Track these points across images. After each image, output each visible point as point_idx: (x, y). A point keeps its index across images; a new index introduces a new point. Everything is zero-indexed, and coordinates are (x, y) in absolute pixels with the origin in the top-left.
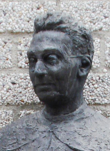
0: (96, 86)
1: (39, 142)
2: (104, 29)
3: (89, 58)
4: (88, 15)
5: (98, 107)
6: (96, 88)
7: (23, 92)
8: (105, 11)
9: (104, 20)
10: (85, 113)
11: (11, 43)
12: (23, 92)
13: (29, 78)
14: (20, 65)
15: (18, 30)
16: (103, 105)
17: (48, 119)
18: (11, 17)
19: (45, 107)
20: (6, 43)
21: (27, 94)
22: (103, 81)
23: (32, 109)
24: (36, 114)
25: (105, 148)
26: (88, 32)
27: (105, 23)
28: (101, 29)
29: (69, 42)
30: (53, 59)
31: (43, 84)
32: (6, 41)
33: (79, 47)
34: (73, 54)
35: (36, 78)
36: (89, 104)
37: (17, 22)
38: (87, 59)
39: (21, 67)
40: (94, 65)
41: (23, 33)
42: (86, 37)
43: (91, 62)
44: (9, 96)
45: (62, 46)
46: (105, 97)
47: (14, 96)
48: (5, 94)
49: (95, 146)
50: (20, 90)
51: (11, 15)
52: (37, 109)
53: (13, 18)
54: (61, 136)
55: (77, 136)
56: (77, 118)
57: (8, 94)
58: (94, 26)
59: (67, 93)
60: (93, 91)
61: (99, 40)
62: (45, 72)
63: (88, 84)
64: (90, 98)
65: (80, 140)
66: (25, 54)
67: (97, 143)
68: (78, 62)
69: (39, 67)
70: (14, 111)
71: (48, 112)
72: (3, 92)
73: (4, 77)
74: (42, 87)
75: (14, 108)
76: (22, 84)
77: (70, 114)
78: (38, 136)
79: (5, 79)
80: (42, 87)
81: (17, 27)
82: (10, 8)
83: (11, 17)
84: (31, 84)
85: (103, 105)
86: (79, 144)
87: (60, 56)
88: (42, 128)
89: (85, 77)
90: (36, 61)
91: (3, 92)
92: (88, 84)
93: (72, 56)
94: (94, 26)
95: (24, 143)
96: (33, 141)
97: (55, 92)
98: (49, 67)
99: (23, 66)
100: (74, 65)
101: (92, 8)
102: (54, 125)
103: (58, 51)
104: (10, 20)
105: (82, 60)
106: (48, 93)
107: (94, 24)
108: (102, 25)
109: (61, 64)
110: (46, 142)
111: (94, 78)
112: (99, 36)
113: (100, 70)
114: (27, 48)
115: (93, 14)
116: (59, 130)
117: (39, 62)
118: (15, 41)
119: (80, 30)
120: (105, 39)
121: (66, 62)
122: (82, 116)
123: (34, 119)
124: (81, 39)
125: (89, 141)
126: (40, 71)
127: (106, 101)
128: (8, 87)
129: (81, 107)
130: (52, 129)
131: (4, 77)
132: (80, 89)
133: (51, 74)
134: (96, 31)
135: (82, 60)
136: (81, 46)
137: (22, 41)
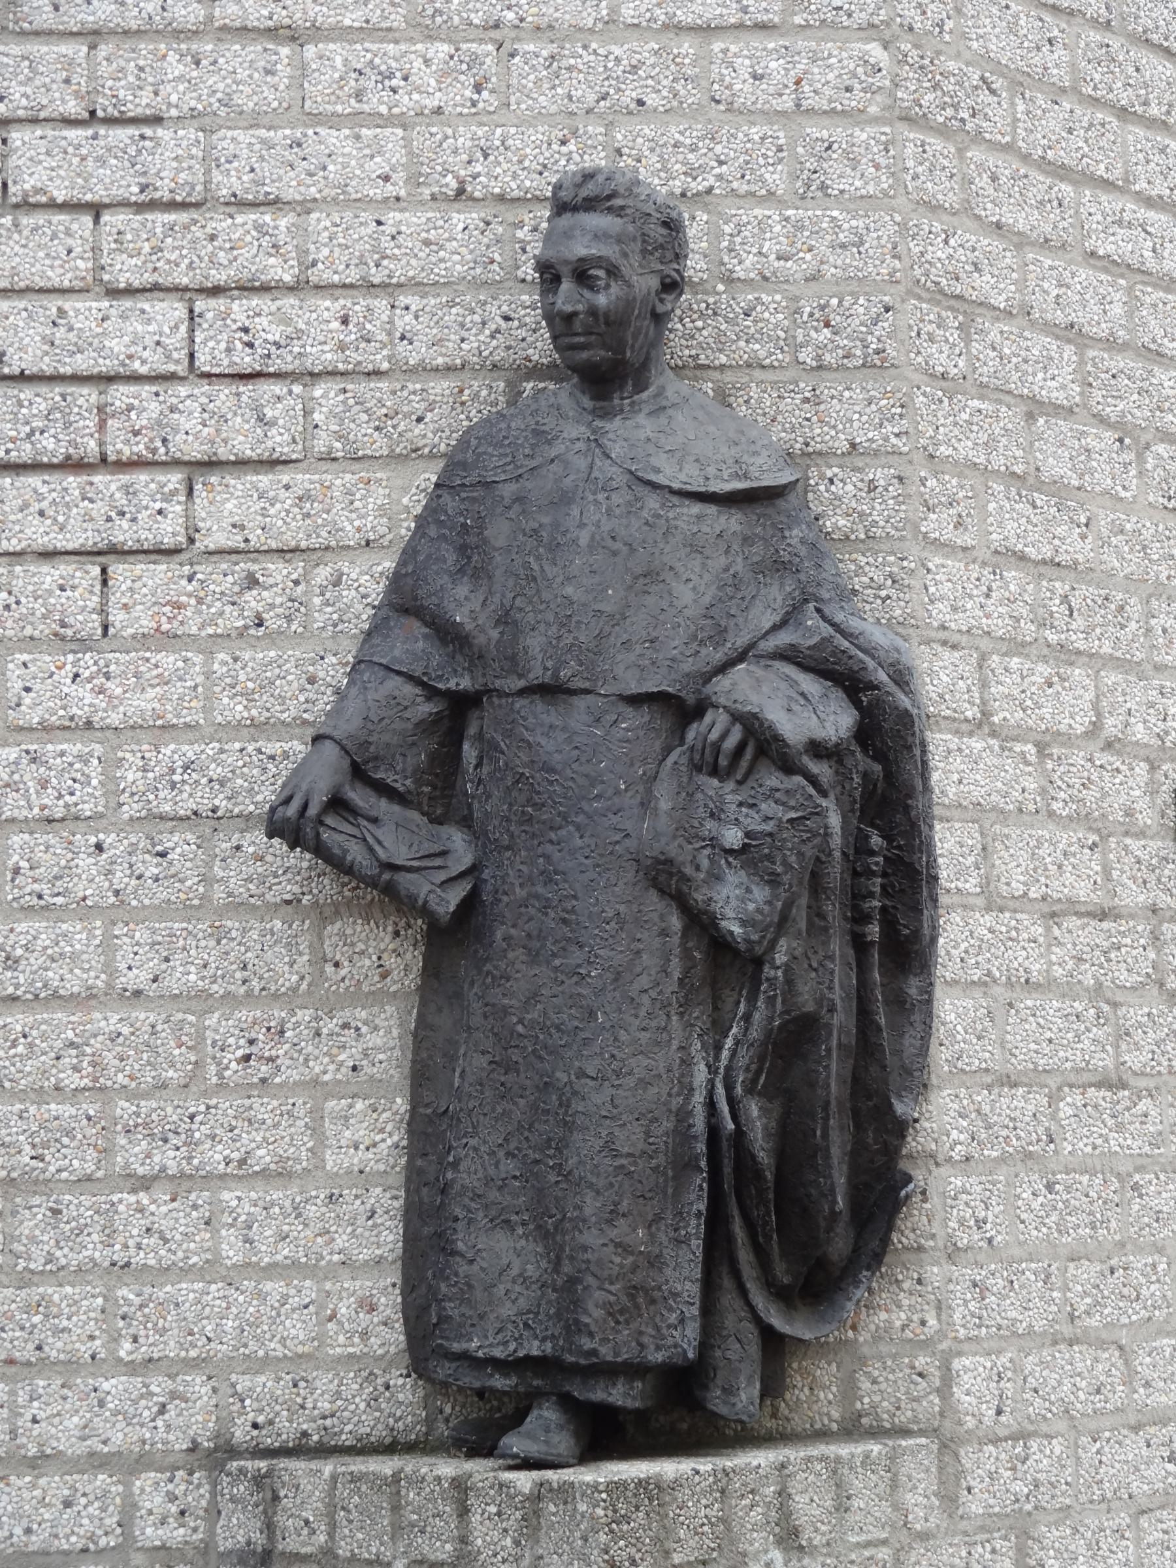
0: (700, 324)
1: (566, 463)
4: (680, 157)
5: (705, 374)
6: (699, 330)
8: (718, 149)
9: (717, 171)
14: (520, 274)
15: (516, 194)
16: (715, 368)
18: (499, 164)
20: (488, 223)
28: (709, 191)
37: (515, 176)
39: (523, 281)
46: (721, 351)
47: (508, 348)
50: (522, 333)
51: (501, 159)
53: (505, 166)
60: (693, 337)
64: (687, 352)
72: (482, 338)
73: (485, 303)
76: (527, 320)
81: (514, 186)
82: (497, 143)
85: (715, 368)
91: (482, 338)
92: (681, 320)
94: (693, 185)
99: (529, 278)
104: (499, 170)
107: (695, 179)
108: (712, 181)
111: (695, 307)
115: (690, 156)
127: (723, 359)
128: (494, 327)
131: (485, 303)
137: (527, 221)
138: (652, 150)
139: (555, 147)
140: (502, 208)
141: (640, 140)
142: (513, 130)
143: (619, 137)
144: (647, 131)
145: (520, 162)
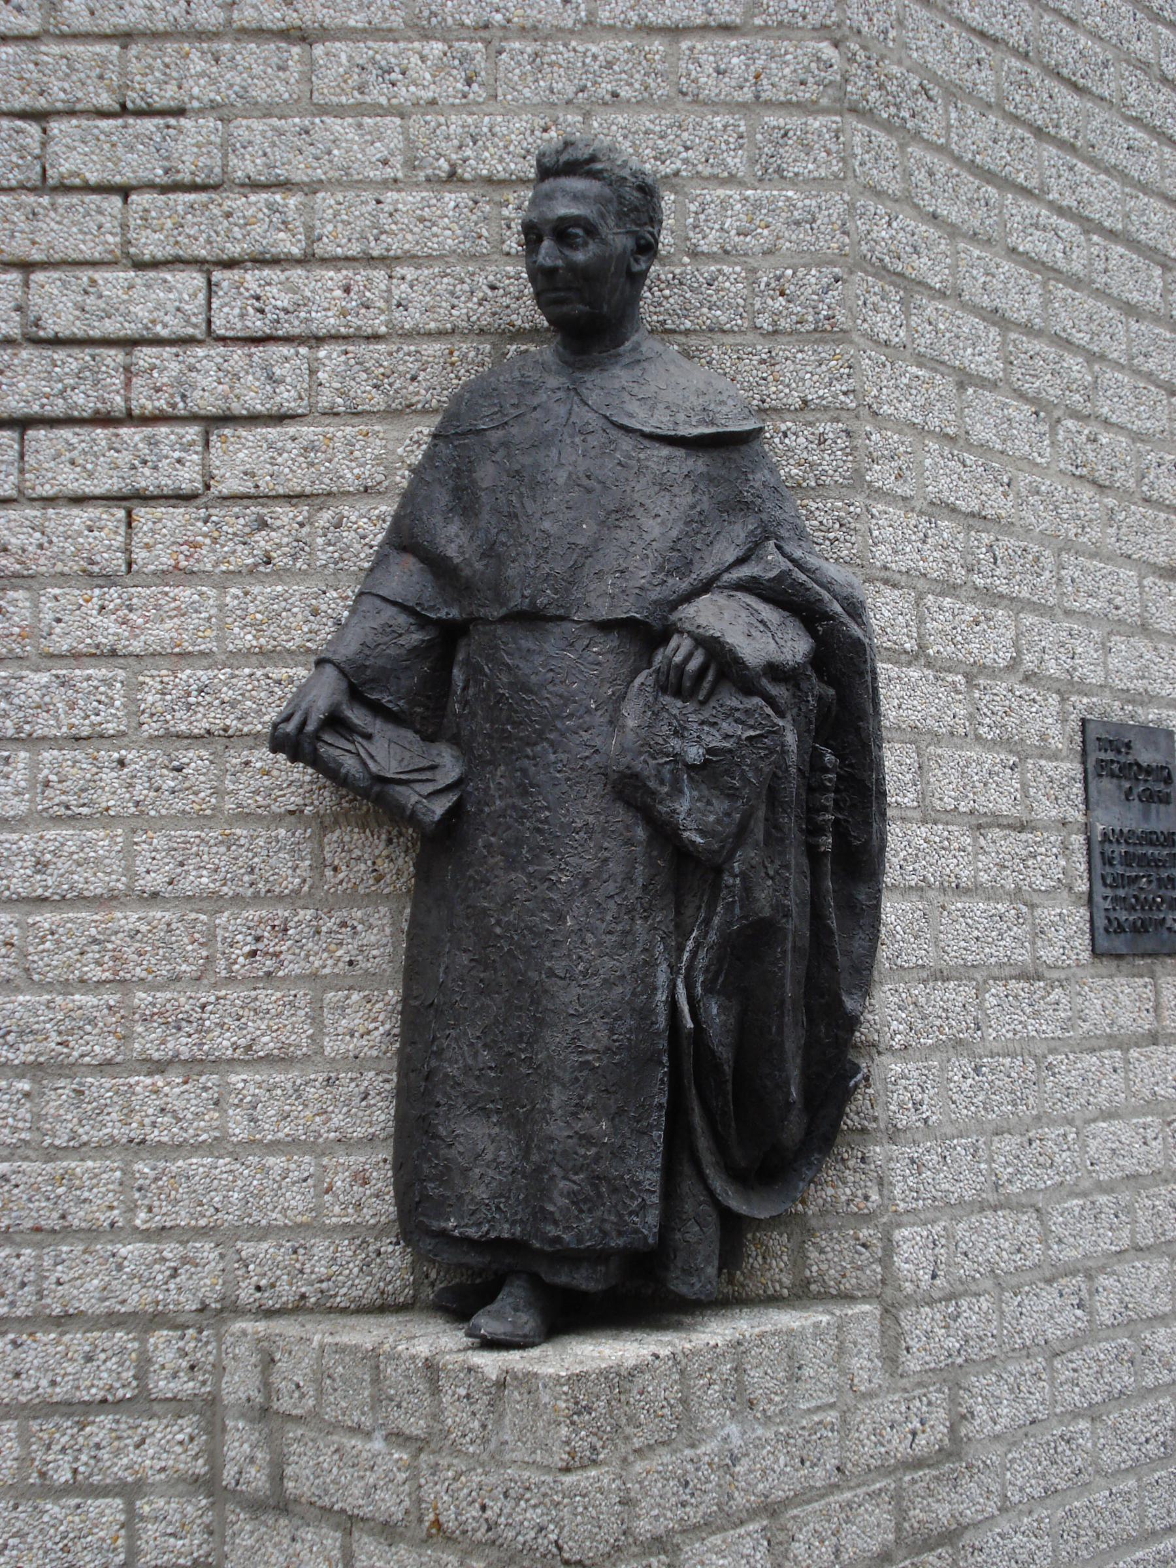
0: (667, 292)
2: (684, 174)
3: (652, 234)
4: (650, 143)
5: (671, 337)
6: (666, 298)
7: (514, 306)
8: (685, 135)
9: (684, 155)
10: (644, 349)
11: (488, 202)
12: (514, 306)
13: (525, 275)
14: (505, 248)
15: (502, 175)
16: (681, 333)
17: (565, 362)
18: (487, 149)
19: (558, 338)
20: (476, 203)
21: (522, 311)
22: (681, 283)
23: (532, 341)
24: (541, 352)
25: (685, 423)
26: (649, 181)
27: (686, 161)
28: (677, 174)
29: (610, 201)
30: (577, 236)
31: (556, 289)
32: (478, 198)
33: (631, 211)
34: (617, 226)
35: (539, 276)
36: (652, 332)
37: (501, 160)
38: (648, 236)
39: (508, 254)
40: (663, 250)
41: (512, 181)
42: (647, 191)
43: (657, 242)
44: (483, 314)
45: (594, 209)
46: (686, 317)
47: (494, 314)
48: (475, 311)
49: (664, 419)
50: (506, 301)
51: (489, 144)
52: (542, 342)
53: (492, 150)
54: (593, 398)
55: (627, 397)
56: (627, 361)
57: (481, 309)
58: (662, 167)
59: (605, 308)
60: (660, 305)
61: (672, 197)
62: (560, 263)
63: (650, 289)
64: (655, 318)
65: (633, 406)
66: (516, 226)
67: (668, 412)
68: (630, 243)
69: (547, 254)
70: (493, 345)
71: (565, 348)
72: (470, 305)
73: (473, 274)
74: (553, 295)
75: (495, 339)
76: (512, 288)
77: (612, 352)
78: (545, 397)
79: (476, 278)
80: (553, 295)
81: (500, 168)
82: (485, 130)
83: (487, 149)
84: (529, 290)
85: (681, 333)
86: (631, 416)
87: (591, 230)
88: (553, 382)
89: (644, 274)
90: (540, 240)
91: (470, 305)
92: (650, 289)
93: (616, 230)
94: (662, 167)
95: (514, 412)
96: (535, 409)
97: (581, 307)
98: (567, 252)
99: (513, 251)
100: (620, 250)
101: (658, 129)
102: (578, 375)
103: (586, 219)
104: (486, 154)
105: (638, 238)
106: (565, 309)
107: (663, 163)
108: (679, 164)
109: (593, 248)
110: (562, 410)
111: (663, 277)
112: (674, 189)
113: (675, 259)
114: (521, 214)
115: (660, 142)
116: (589, 385)
117: (546, 243)
118: (497, 198)
119: (634, 175)
120: (686, 195)
121: (604, 242)
122: (638, 357)
123: (536, 362)
124: (636, 194)
125: (653, 408)
126: (549, 263)
127: (688, 324)
128: (481, 295)
129: (635, 338)
130: (574, 382)
131: (473, 274)
132: (636, 297)
133: (572, 267)
134: (666, 176)
135: (638, 238)
136: (636, 209)
137: (511, 199)
138: (625, 137)
139: (537, 133)
140: (490, 189)
141: (614, 128)
142: (499, 119)
143: (595, 124)
144: (620, 119)
145: (506, 147)
